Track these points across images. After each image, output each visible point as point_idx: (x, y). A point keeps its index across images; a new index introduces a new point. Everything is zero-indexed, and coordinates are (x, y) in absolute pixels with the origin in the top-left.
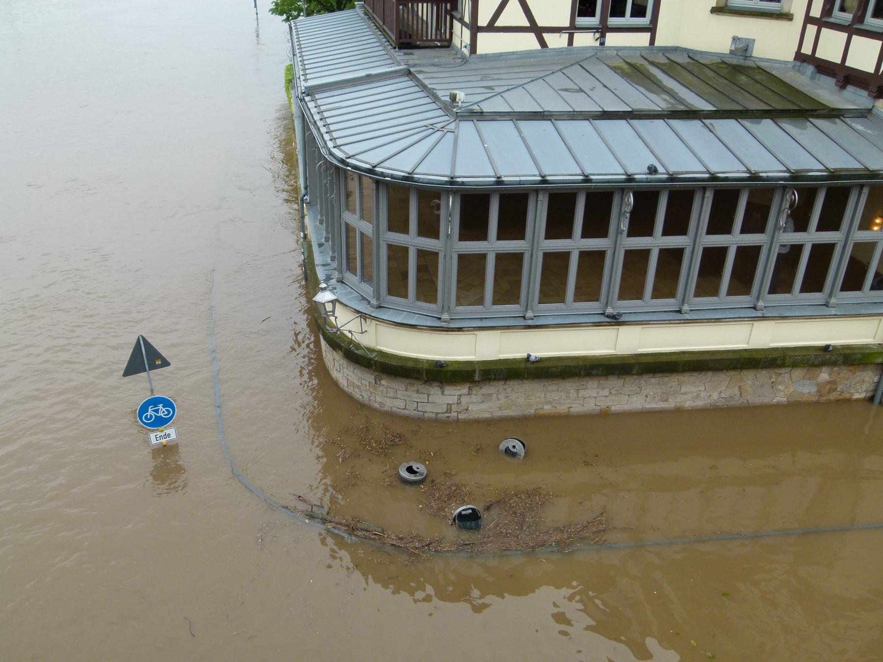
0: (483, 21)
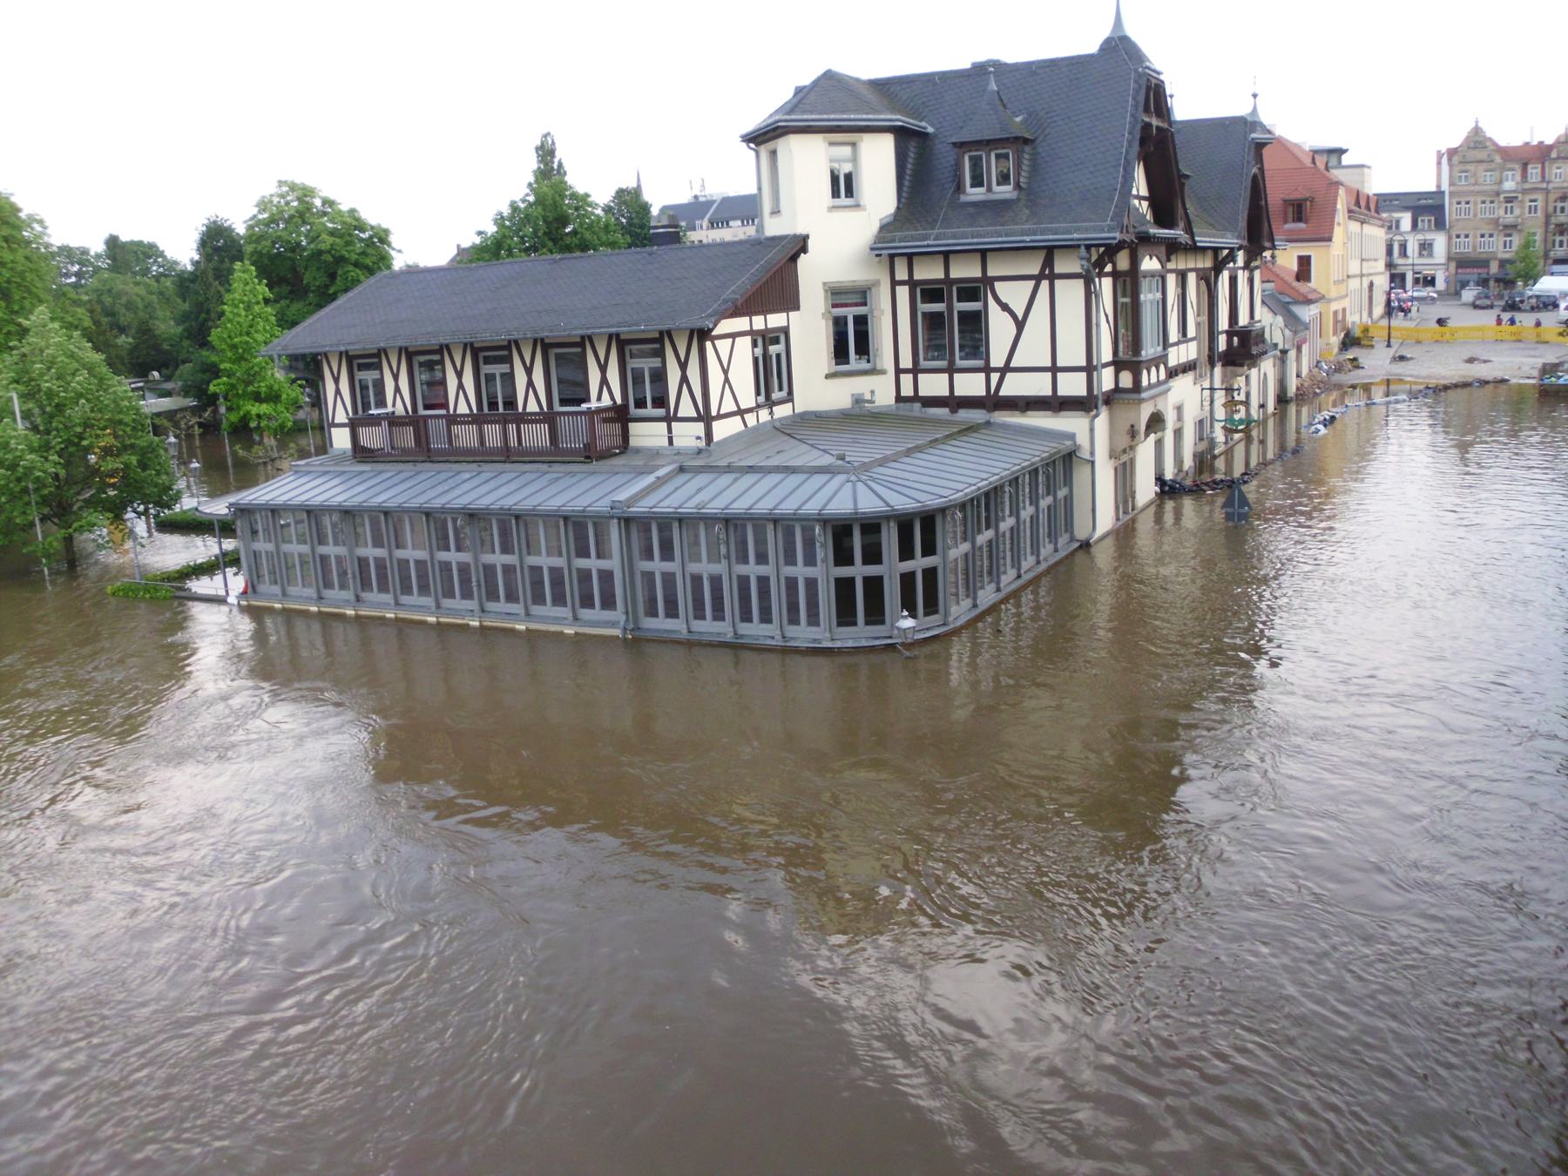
0: (714, 413)
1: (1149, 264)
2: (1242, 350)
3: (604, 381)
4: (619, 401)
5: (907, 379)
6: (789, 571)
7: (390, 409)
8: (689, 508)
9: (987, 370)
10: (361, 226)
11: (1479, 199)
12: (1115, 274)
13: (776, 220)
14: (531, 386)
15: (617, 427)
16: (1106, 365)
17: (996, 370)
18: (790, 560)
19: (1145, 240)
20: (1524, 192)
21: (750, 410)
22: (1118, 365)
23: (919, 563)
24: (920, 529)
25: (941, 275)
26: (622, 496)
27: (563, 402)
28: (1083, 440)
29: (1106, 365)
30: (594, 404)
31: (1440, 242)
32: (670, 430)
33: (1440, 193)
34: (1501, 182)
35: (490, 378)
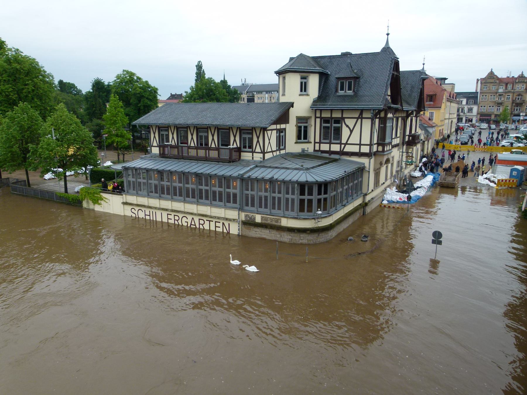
1: (390, 115)
2: (413, 141)
3: (235, 140)
4: (239, 146)
5: (317, 145)
6: (287, 196)
7: (170, 143)
8: (260, 177)
9: (341, 144)
10: (149, 86)
11: (490, 95)
12: (380, 118)
13: (284, 97)
14: (213, 141)
15: (238, 153)
16: (375, 144)
17: (343, 144)
18: (288, 193)
19: (390, 108)
20: (506, 93)
21: (274, 151)
22: (378, 144)
23: (323, 196)
24: (323, 186)
25: (329, 116)
26: (242, 172)
27: (222, 145)
28: (367, 165)
29: (375, 144)
30: (231, 147)
31: (475, 109)
32: (253, 155)
33: (477, 93)
34: (498, 90)
35: (201, 137)
